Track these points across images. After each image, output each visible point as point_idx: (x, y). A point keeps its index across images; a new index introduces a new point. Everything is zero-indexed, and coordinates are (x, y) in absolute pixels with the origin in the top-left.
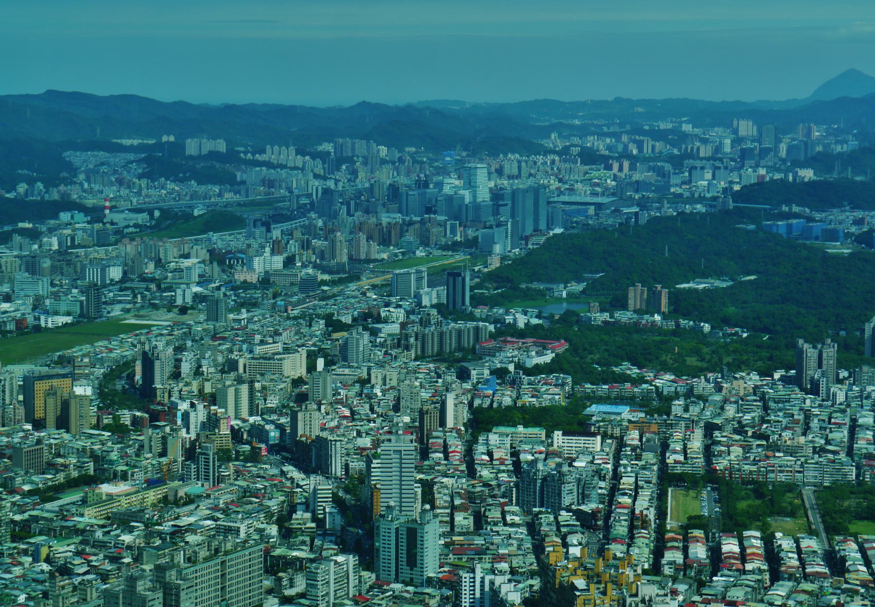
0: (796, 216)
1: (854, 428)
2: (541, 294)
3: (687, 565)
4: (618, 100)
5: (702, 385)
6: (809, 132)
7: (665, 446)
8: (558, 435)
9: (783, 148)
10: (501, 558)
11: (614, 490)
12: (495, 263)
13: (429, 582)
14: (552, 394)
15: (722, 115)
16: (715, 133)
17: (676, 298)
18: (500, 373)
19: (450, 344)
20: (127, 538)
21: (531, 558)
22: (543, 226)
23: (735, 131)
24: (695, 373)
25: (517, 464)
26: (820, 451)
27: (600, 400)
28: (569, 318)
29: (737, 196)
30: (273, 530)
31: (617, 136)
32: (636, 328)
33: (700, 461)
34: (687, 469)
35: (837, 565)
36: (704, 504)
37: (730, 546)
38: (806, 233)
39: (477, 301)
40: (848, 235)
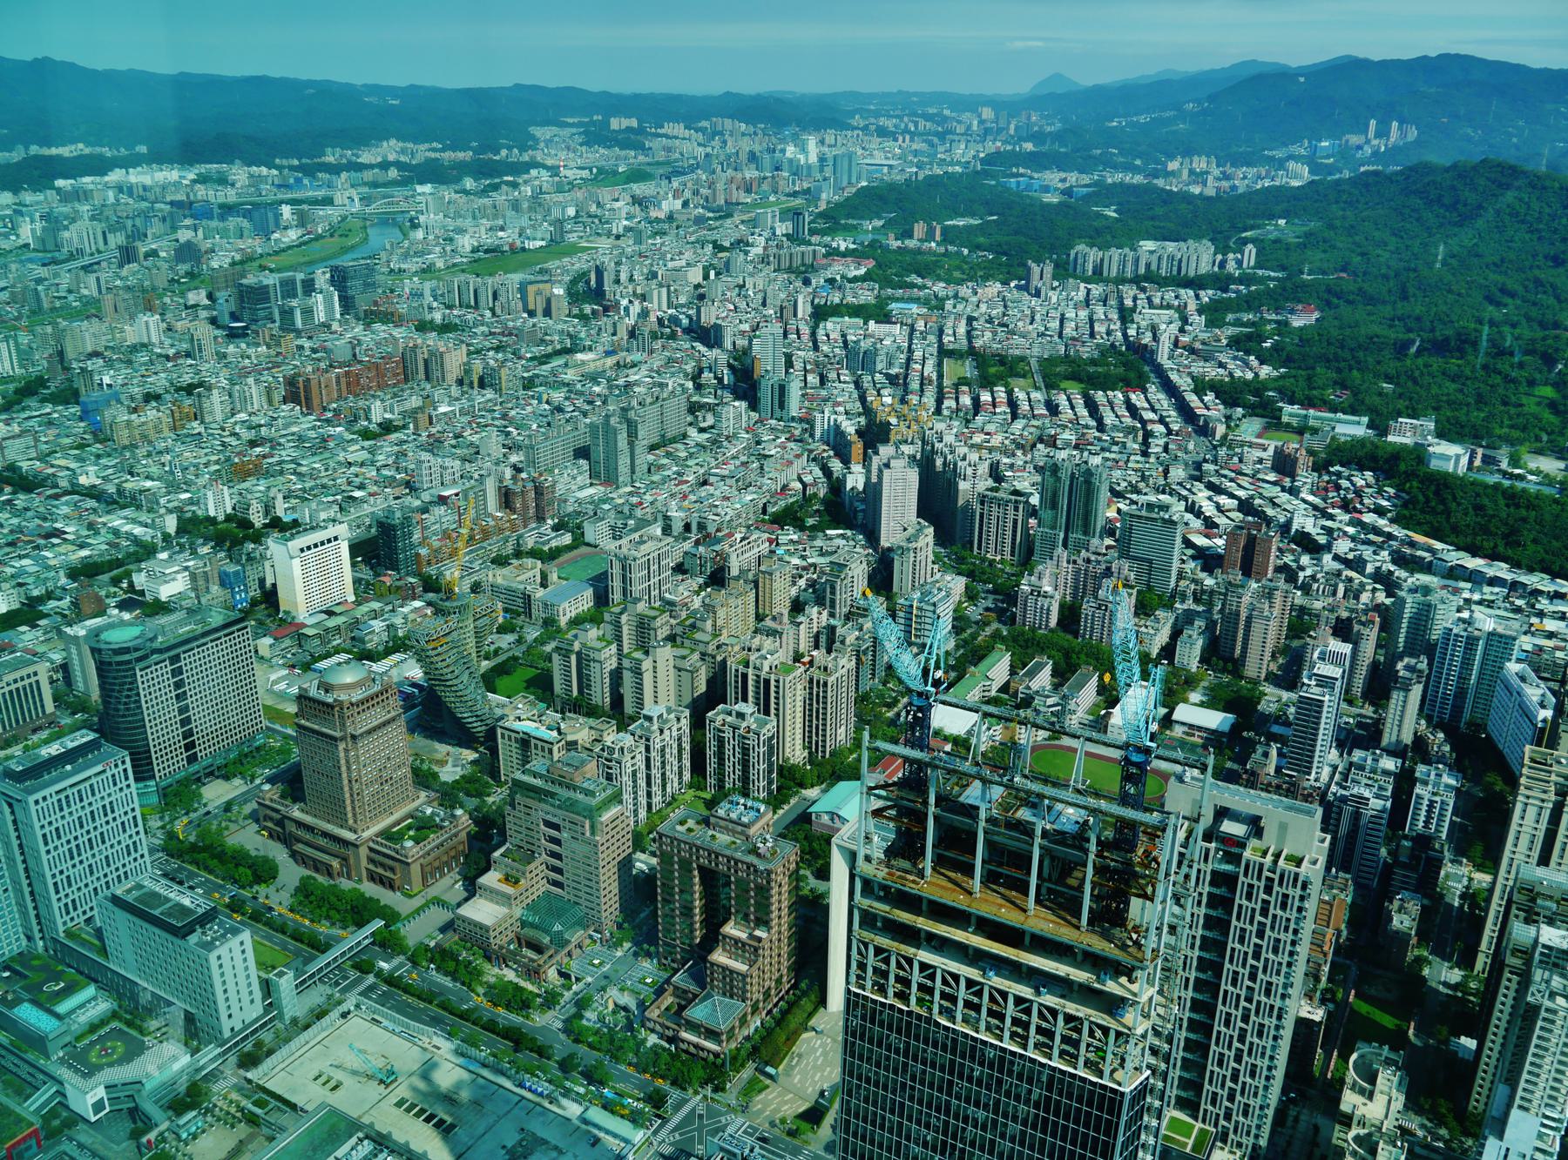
0: (1022, 175)
1: (1062, 319)
2: (855, 227)
3: (958, 410)
4: (900, 92)
5: (964, 291)
6: (1029, 118)
7: (941, 332)
8: (872, 323)
9: (1012, 127)
10: (839, 404)
11: (909, 360)
12: (823, 206)
13: (793, 419)
14: (866, 296)
15: (971, 104)
16: (966, 116)
17: (945, 231)
18: (831, 281)
19: (797, 262)
20: (597, 389)
21: (858, 404)
22: (854, 180)
23: (980, 116)
24: (960, 282)
25: (845, 342)
26: (1043, 335)
27: (898, 300)
28: (872, 244)
29: (982, 161)
30: (690, 385)
31: (900, 117)
32: (919, 251)
33: (965, 342)
34: (956, 346)
35: (1053, 409)
36: (968, 369)
37: (986, 397)
38: (1029, 187)
39: (813, 232)
40: (1056, 189)
